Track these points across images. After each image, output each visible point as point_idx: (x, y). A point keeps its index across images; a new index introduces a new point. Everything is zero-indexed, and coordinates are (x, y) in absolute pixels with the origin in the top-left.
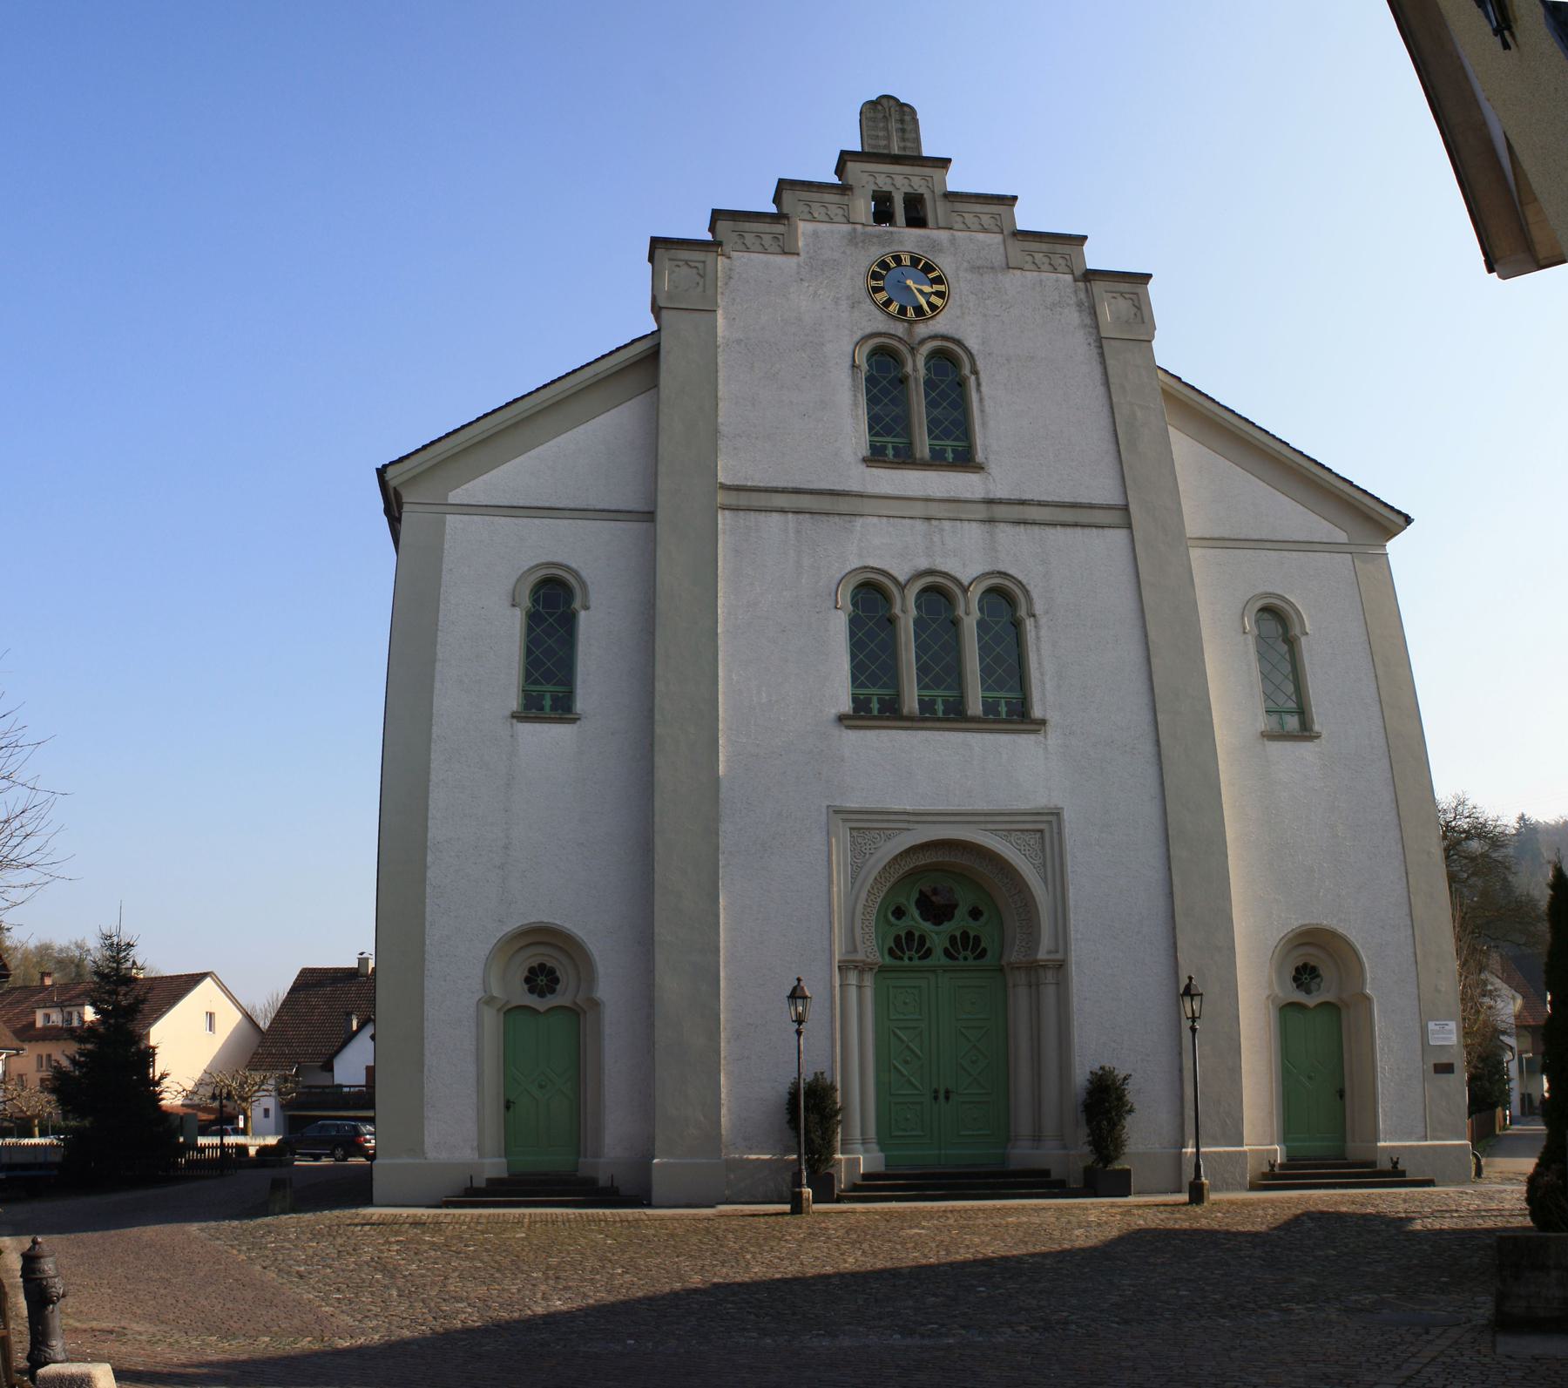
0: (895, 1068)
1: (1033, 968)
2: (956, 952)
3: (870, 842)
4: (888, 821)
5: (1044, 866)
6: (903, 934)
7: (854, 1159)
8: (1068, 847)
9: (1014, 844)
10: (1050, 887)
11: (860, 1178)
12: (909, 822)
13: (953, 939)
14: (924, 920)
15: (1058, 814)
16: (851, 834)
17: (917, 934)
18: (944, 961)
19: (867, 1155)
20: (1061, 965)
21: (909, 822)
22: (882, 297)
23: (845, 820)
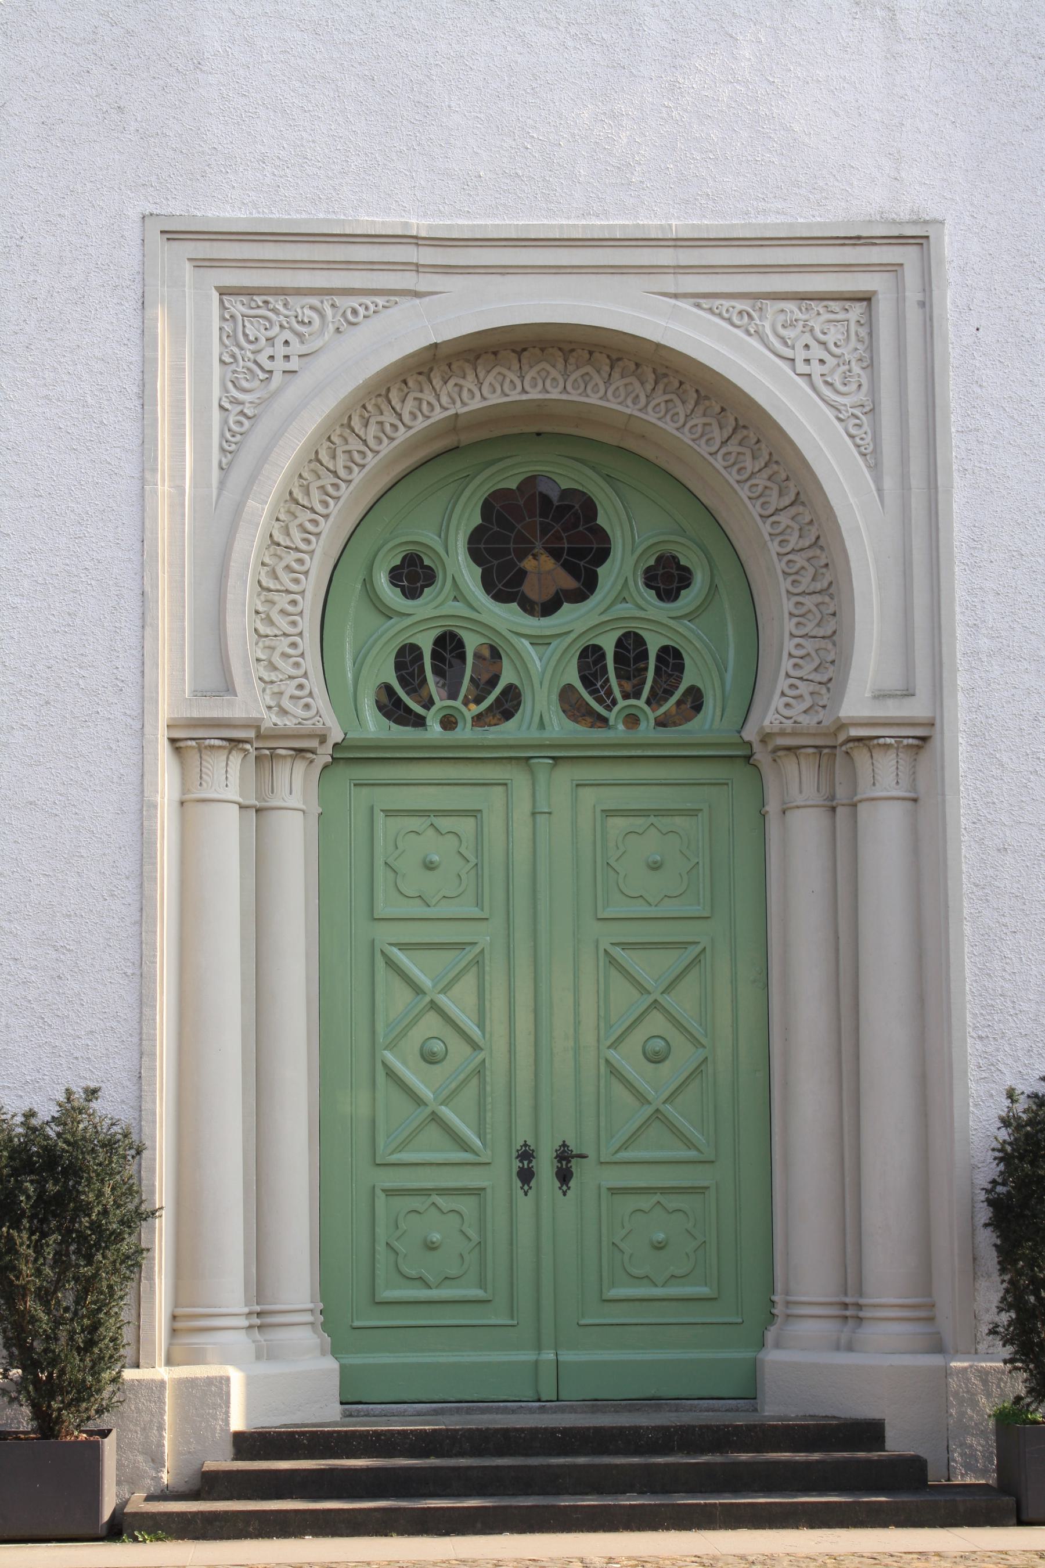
0: (391, 1074)
2: (600, 701)
3: (287, 335)
4: (348, 265)
5: (873, 411)
6: (426, 644)
7: (210, 1381)
8: (954, 352)
9: (772, 339)
10: (889, 483)
11: (229, 1449)
12: (417, 268)
15: (921, 241)
16: (221, 301)
17: (472, 643)
19: (263, 1369)
20: (924, 739)
21: (417, 268)
23: (200, 264)
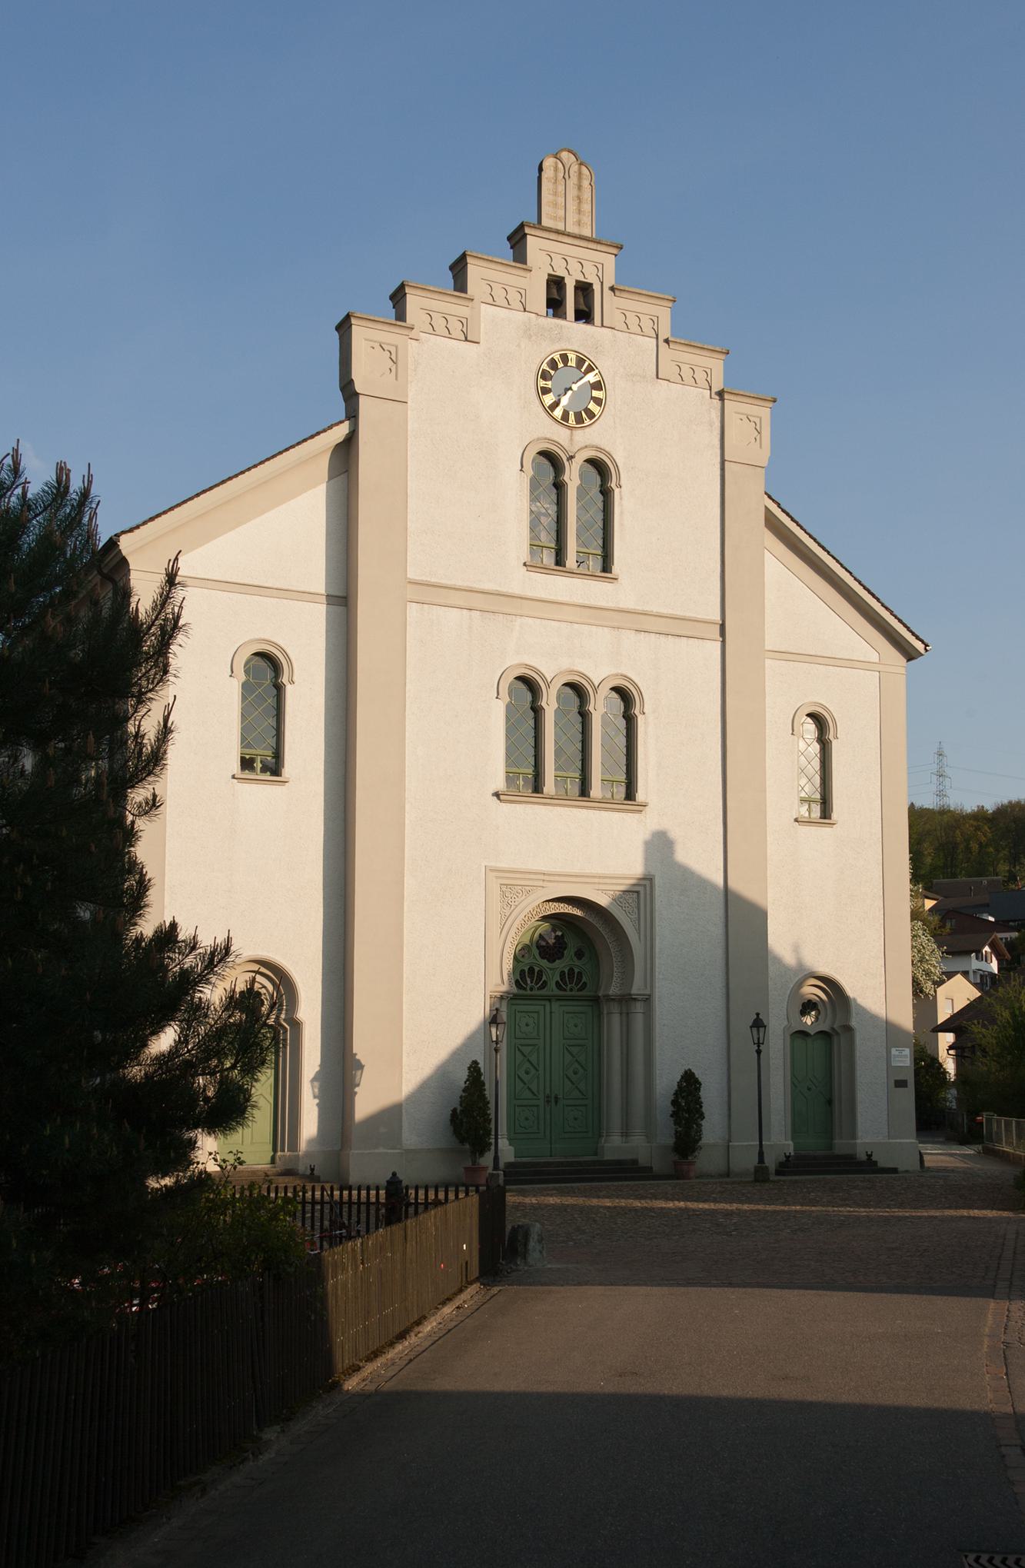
1: (626, 1000)
13: (562, 974)
14: (542, 958)
17: (537, 969)
18: (557, 992)
22: (549, 399)
